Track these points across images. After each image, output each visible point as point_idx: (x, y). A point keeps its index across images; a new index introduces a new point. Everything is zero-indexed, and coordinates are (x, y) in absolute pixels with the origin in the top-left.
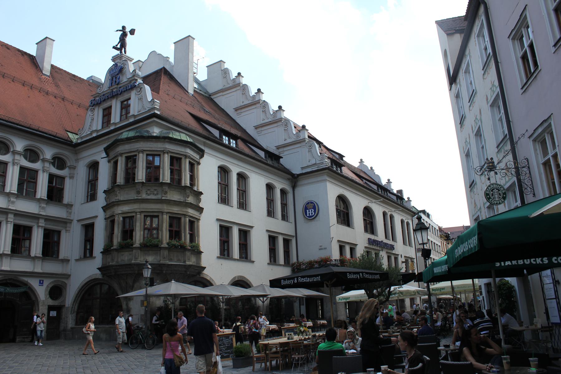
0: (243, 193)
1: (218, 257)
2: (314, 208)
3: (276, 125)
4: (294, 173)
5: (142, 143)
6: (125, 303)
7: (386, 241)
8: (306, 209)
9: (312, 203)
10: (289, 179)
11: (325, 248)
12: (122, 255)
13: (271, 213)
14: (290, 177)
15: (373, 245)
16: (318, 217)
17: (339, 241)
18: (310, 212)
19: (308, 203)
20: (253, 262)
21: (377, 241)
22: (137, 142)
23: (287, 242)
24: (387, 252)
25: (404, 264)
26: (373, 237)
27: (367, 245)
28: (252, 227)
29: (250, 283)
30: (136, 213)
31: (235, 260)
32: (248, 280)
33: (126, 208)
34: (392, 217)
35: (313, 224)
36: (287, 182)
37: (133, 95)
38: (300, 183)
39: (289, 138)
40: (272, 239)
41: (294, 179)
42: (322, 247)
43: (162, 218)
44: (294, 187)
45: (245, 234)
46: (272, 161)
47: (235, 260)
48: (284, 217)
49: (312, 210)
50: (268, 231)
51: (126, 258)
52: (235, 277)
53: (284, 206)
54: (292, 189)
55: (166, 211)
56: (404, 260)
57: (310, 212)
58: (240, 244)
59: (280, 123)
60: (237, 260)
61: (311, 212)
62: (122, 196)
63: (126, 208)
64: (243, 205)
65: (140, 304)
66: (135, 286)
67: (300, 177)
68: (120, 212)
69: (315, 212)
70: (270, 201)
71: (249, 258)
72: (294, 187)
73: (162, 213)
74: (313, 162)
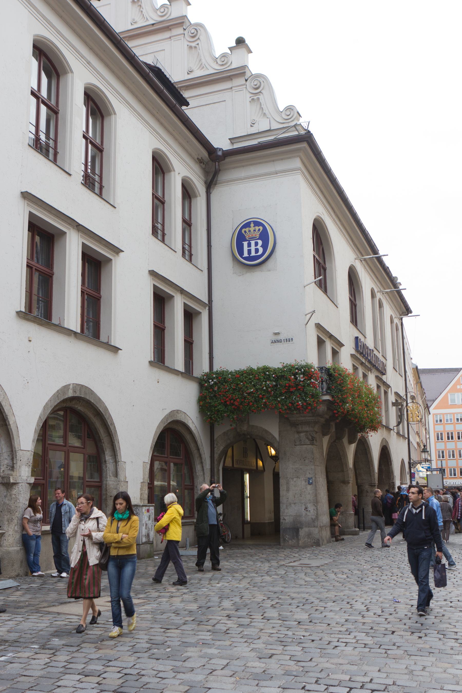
0: (97, 149)
1: (19, 313)
2: (264, 236)
3: (166, 35)
4: (216, 145)
7: (376, 352)
8: (241, 238)
9: (257, 224)
10: (200, 161)
11: (289, 340)
13: (158, 230)
14: (204, 154)
15: (361, 354)
16: (270, 263)
17: (319, 326)
18: (253, 248)
19: (247, 225)
20: (115, 350)
21: (367, 348)
23: (190, 316)
24: (377, 377)
25: (394, 408)
26: (361, 337)
27: (353, 352)
28: (117, 251)
29: (106, 409)
31: (69, 332)
32: (100, 399)
34: (381, 305)
35: (257, 276)
36: (197, 168)
38: (223, 177)
39: (202, 67)
40: (161, 301)
41: (215, 163)
42: (281, 337)
44: (210, 185)
45: (95, 265)
46: (165, 95)
47: (69, 332)
48: (188, 253)
49: (253, 246)
50: (153, 273)
52: (66, 387)
53: (187, 224)
54: (204, 190)
56: (394, 401)
57: (253, 248)
58: (82, 292)
59: (180, 31)
60: (75, 333)
61: (253, 247)
64: (94, 181)
67: (228, 160)
69: (265, 246)
70: (159, 202)
71: (103, 338)
72: (210, 185)
74: (263, 125)
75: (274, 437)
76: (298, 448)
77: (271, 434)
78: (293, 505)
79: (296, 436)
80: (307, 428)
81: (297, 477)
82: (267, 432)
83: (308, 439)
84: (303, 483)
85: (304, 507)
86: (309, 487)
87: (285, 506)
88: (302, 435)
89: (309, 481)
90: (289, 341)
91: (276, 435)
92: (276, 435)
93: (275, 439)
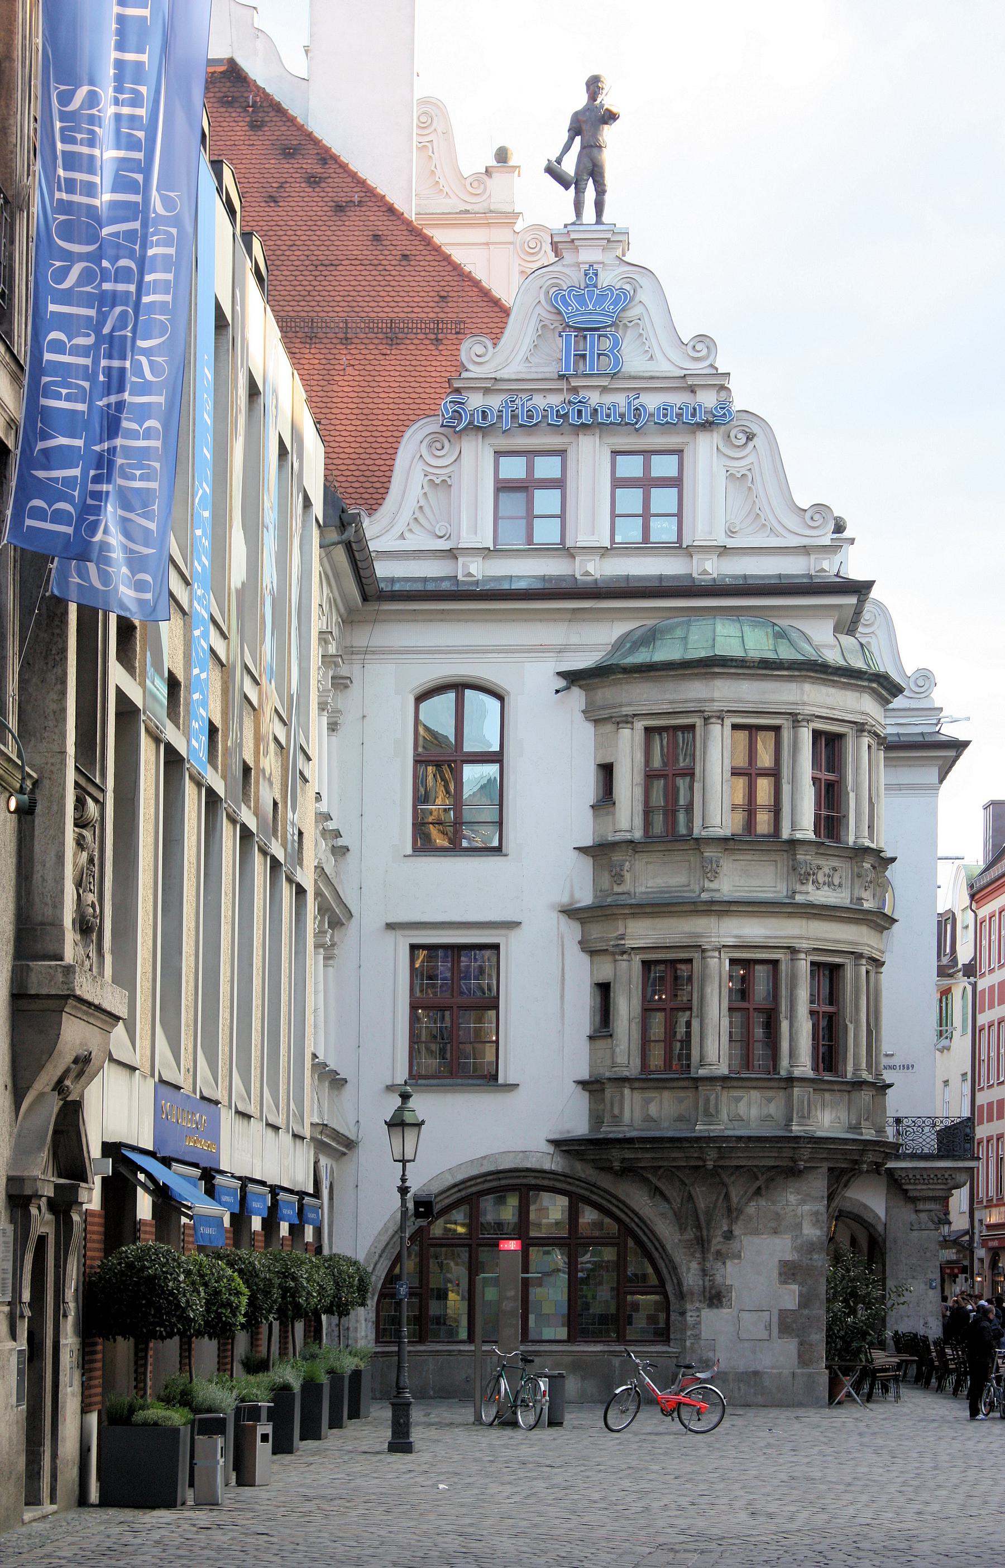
5: (807, 687)
6: (694, 1265)
12: (738, 1100)
22: (790, 678)
30: (793, 950)
33: (754, 930)
37: (705, 452)
43: (857, 977)
51: (754, 1112)
55: (866, 951)
62: (733, 880)
63: (754, 930)
65: (775, 1274)
66: (751, 1209)
68: (731, 941)
73: (860, 956)
75: (877, 1215)
76: (915, 1233)
77: (872, 1211)
78: (906, 1319)
79: (914, 1216)
80: (929, 1206)
81: (913, 1278)
82: (866, 1207)
83: (932, 1221)
84: (922, 1286)
85: (922, 1322)
86: (931, 1292)
87: (893, 1320)
88: (923, 1216)
89: (931, 1284)
90: (908, 1068)
91: (881, 1212)
92: (881, 1212)
93: (879, 1218)
